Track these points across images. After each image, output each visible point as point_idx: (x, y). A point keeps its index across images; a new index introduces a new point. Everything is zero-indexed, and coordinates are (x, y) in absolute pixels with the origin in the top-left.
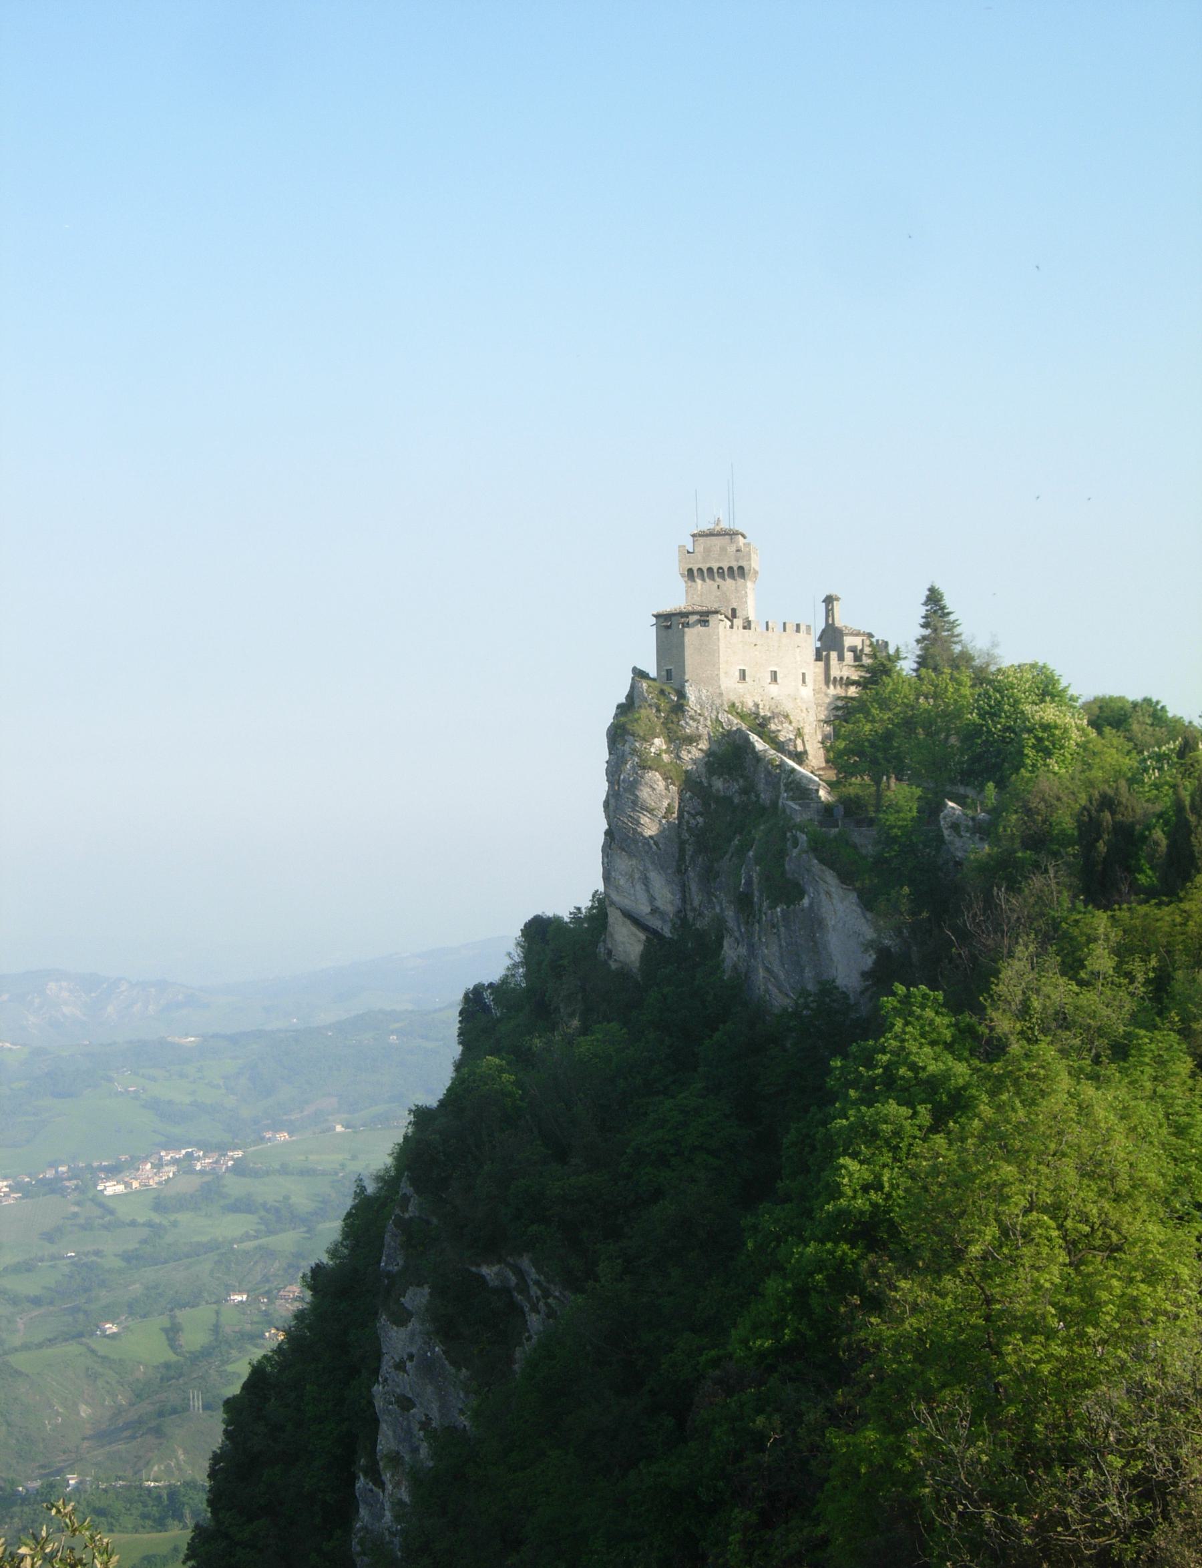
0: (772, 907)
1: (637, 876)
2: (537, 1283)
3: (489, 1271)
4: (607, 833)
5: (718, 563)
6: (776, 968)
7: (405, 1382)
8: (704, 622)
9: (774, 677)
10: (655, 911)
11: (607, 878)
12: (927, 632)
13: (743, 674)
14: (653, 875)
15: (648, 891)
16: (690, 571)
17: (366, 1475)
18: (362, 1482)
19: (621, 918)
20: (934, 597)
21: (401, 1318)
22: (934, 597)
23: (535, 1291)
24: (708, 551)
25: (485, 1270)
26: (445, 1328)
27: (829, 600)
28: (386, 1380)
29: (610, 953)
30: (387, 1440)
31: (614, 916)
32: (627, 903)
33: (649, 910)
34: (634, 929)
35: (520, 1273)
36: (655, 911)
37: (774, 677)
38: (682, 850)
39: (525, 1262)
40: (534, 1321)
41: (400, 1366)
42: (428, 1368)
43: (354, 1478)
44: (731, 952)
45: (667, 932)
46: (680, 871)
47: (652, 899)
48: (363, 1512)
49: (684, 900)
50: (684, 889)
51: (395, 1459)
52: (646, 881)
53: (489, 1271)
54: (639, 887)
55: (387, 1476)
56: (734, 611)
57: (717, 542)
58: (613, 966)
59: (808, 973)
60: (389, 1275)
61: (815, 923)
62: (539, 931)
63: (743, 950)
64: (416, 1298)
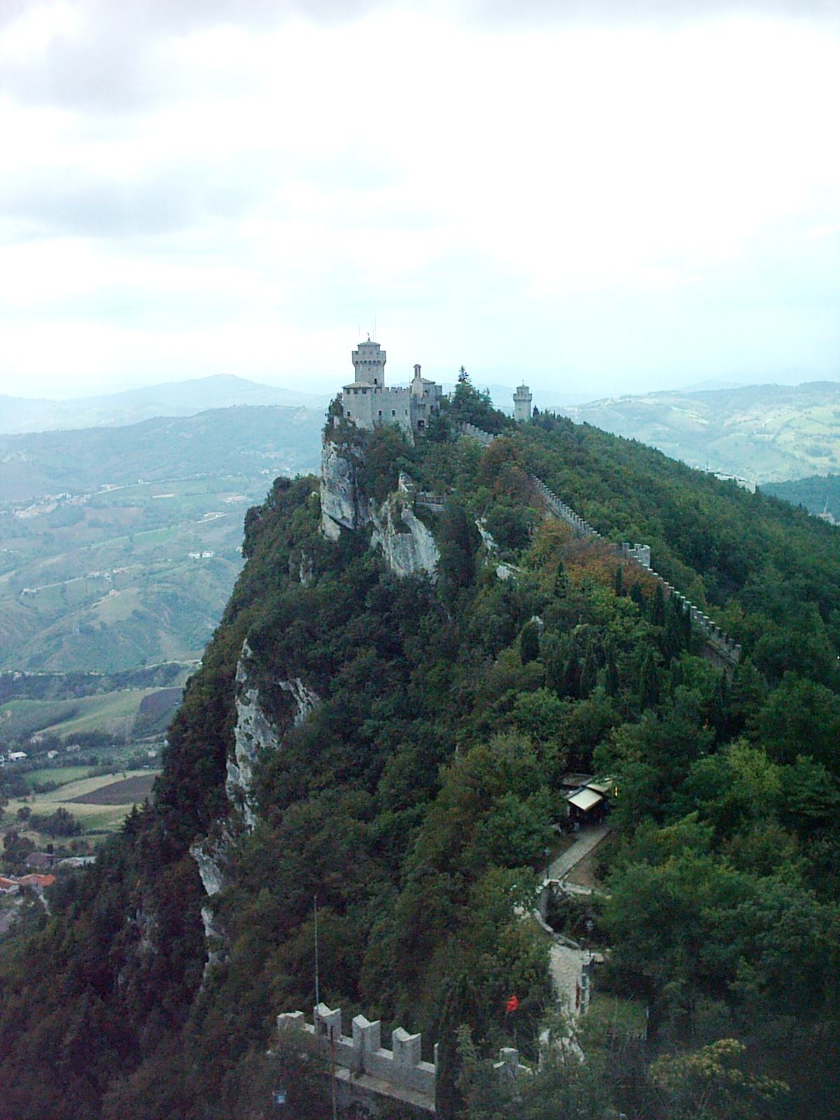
0: (397, 533)
1: (336, 502)
2: (303, 691)
5: (369, 358)
7: (250, 729)
8: (364, 393)
9: (394, 412)
10: (343, 517)
12: (460, 383)
13: (380, 412)
14: (342, 503)
15: (340, 509)
16: (357, 362)
17: (231, 761)
18: (228, 764)
19: (329, 519)
20: (463, 369)
22: (463, 369)
23: (301, 693)
26: (266, 708)
27: (417, 368)
28: (240, 727)
29: (323, 532)
30: (240, 749)
32: (331, 514)
33: (341, 517)
34: (334, 524)
35: (296, 686)
36: (343, 517)
37: (394, 412)
39: (298, 680)
40: (301, 705)
41: (247, 721)
44: (375, 539)
45: (349, 526)
46: (355, 500)
47: (342, 513)
48: (230, 778)
49: (356, 514)
50: (356, 509)
51: (244, 758)
52: (340, 505)
54: (337, 507)
55: (240, 764)
56: (376, 380)
57: (367, 350)
58: (325, 538)
59: (411, 562)
60: (240, 683)
61: (414, 541)
62: (282, 484)
64: (252, 694)
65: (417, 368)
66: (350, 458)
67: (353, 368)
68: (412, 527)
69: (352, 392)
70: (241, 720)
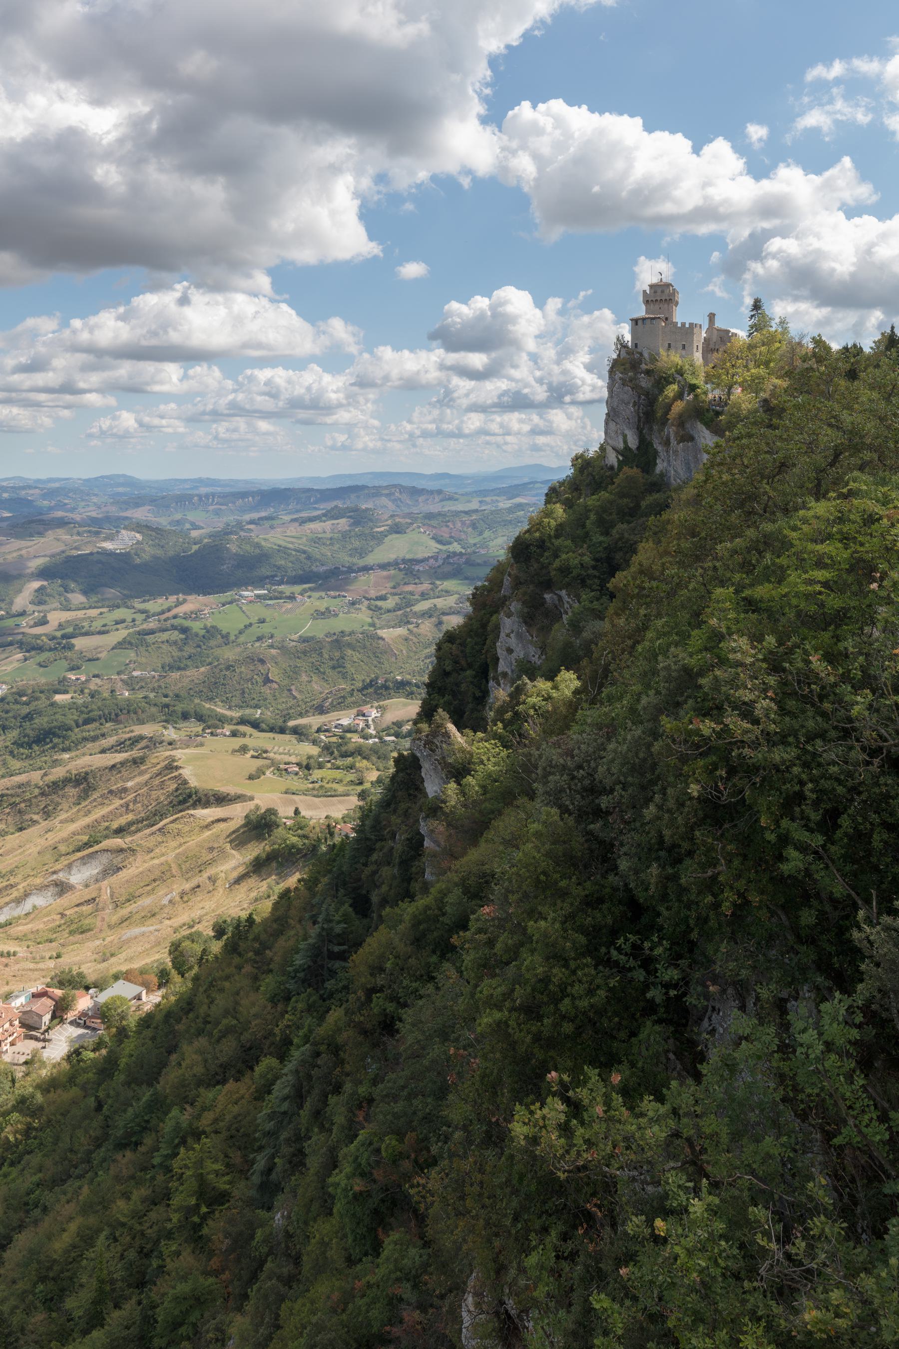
3: (547, 596)
4: (608, 415)
6: (679, 471)
11: (606, 433)
18: (491, 683)
21: (509, 616)
23: (566, 606)
24: (655, 292)
25: (546, 596)
26: (528, 619)
30: (502, 667)
31: (609, 449)
35: (560, 598)
38: (639, 421)
39: (563, 593)
41: (508, 635)
42: (519, 636)
43: (487, 682)
44: (660, 466)
51: (505, 675)
53: (547, 596)
63: (665, 464)
64: (515, 606)
65: (712, 317)
66: (636, 387)
67: (644, 307)
68: (696, 436)
69: (640, 322)
70: (502, 635)
